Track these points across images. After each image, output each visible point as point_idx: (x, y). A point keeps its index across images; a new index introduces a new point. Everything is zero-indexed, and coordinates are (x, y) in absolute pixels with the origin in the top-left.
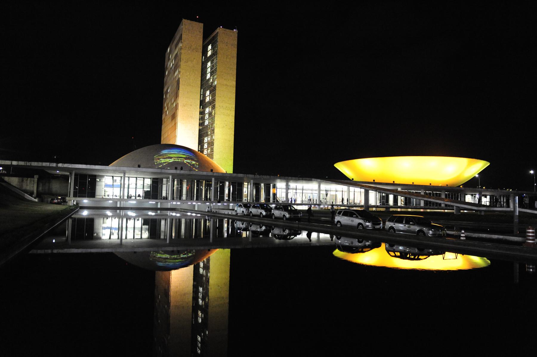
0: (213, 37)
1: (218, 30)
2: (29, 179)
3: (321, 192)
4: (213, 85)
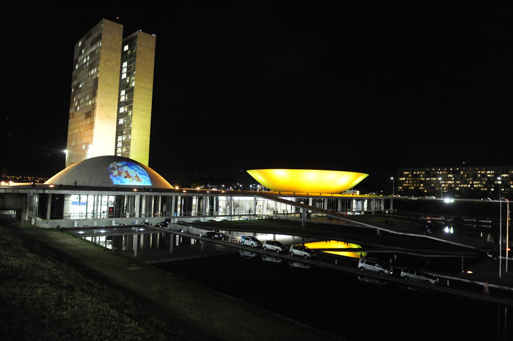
0: (131, 38)
1: (137, 33)
4: (130, 85)
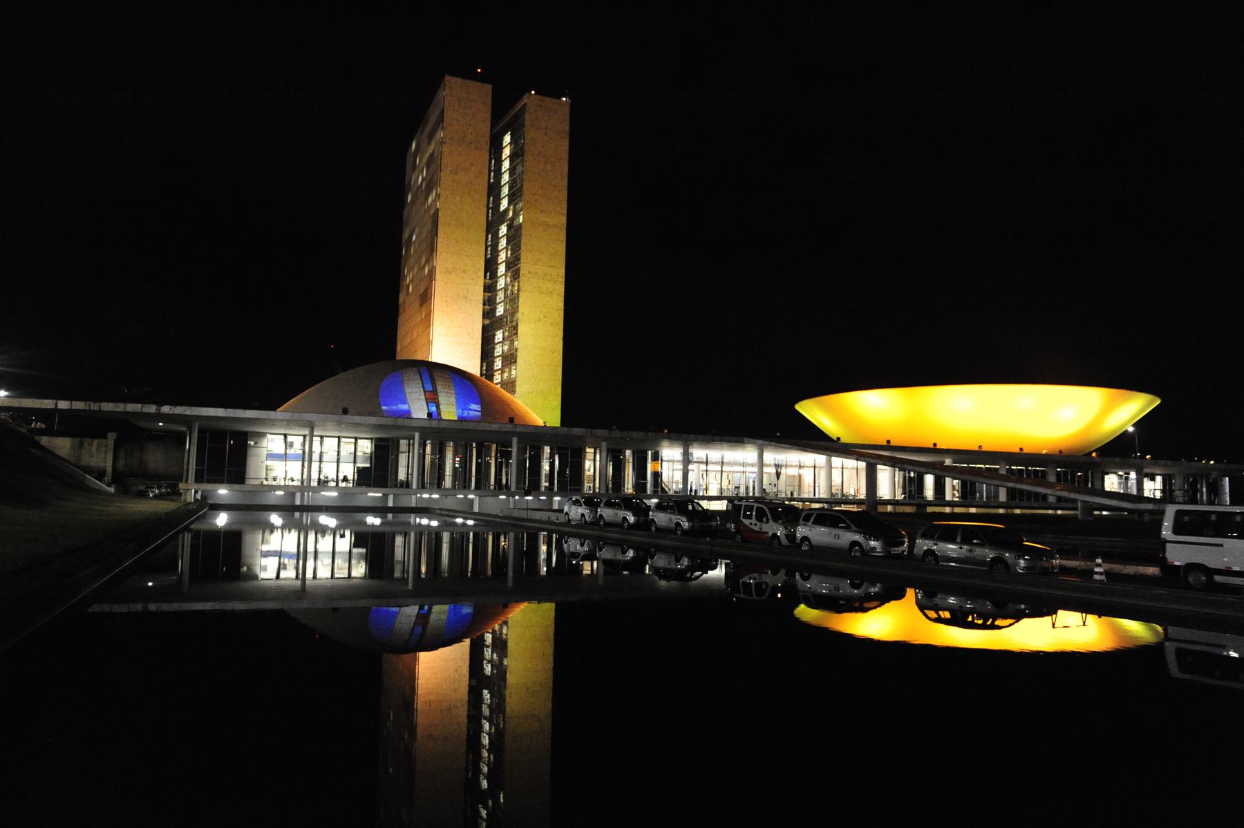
1: (525, 100)
2: (96, 441)
3: (765, 470)
4: (516, 223)
